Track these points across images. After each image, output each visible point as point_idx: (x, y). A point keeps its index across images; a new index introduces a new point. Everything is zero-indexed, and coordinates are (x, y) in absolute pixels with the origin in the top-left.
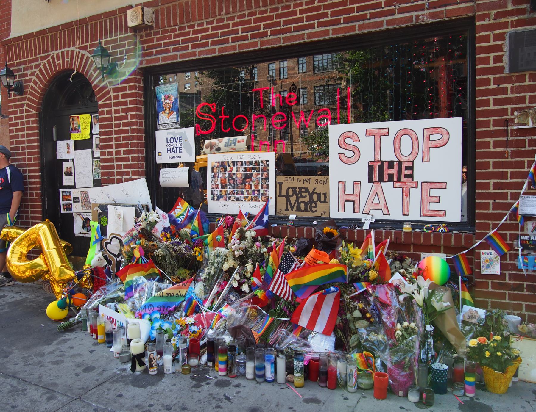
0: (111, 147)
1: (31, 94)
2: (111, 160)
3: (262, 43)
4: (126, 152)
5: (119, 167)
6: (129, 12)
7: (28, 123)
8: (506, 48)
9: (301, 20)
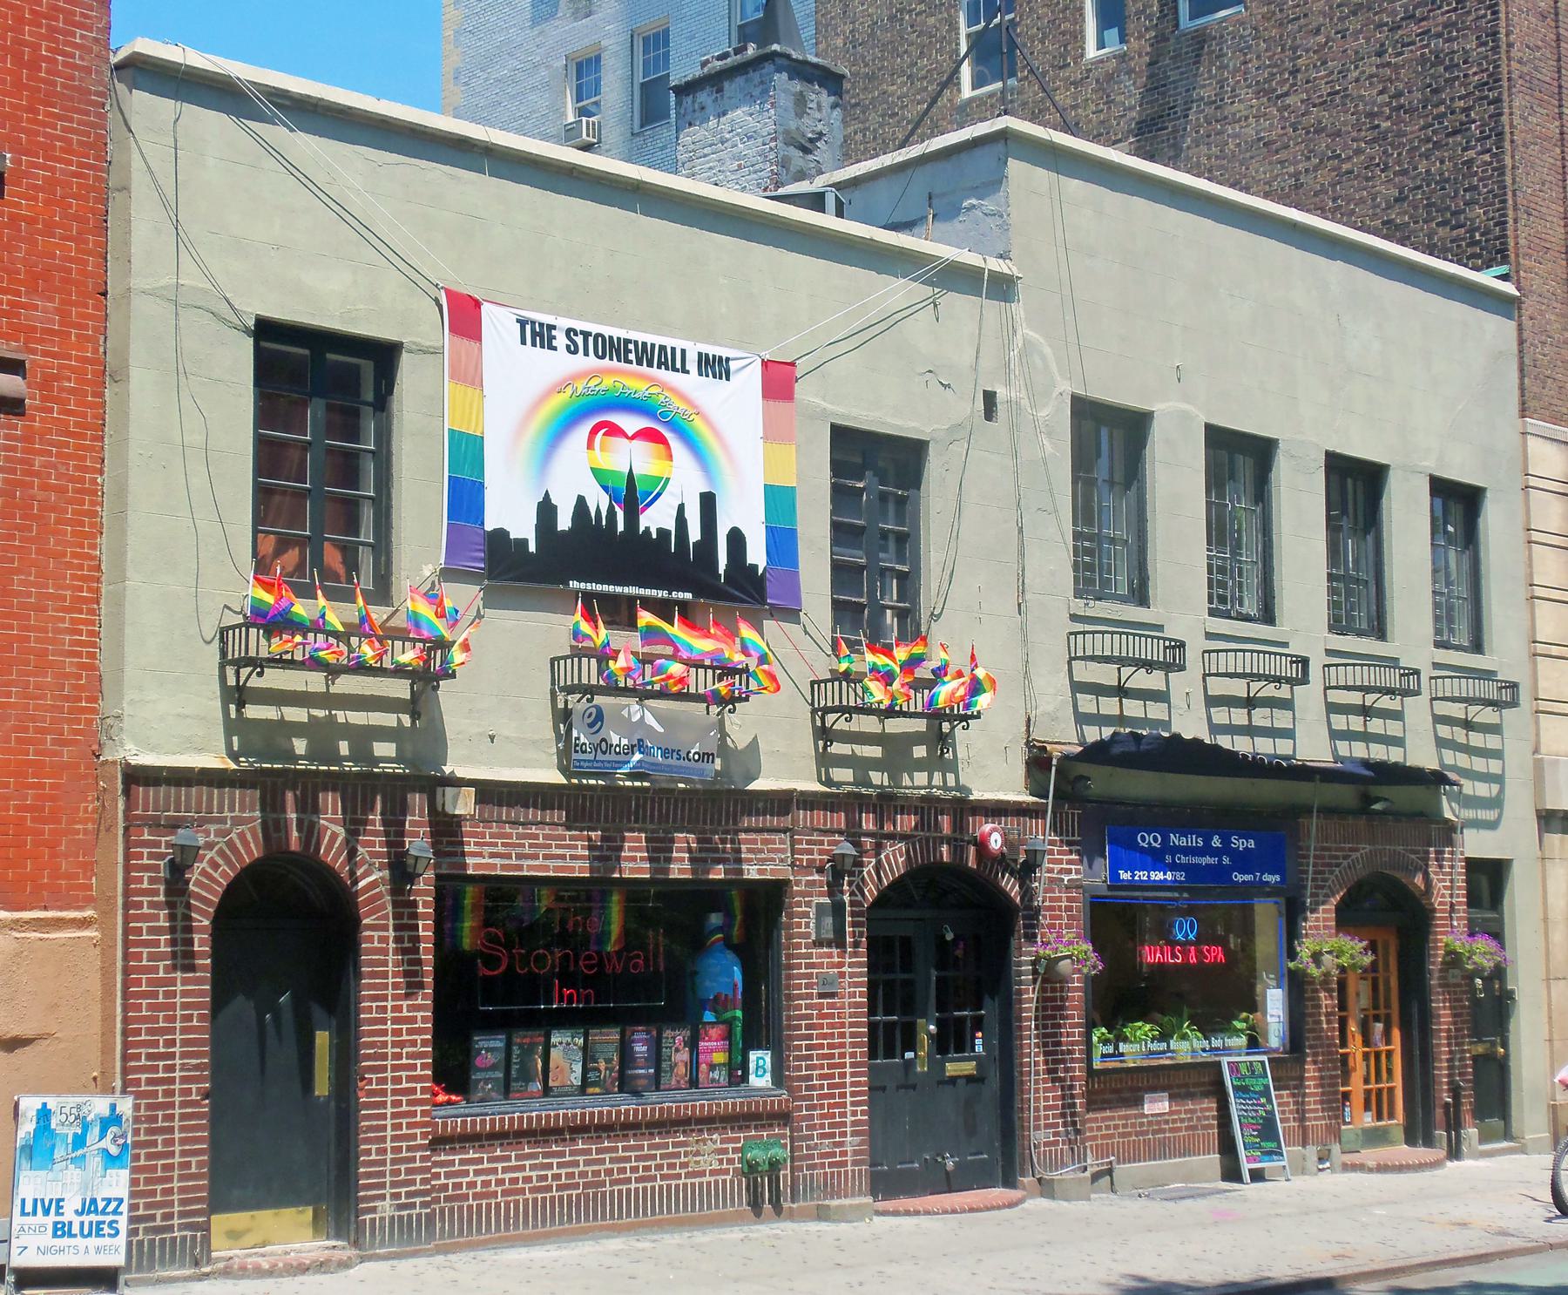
0: (385, 998)
5: (397, 1033)
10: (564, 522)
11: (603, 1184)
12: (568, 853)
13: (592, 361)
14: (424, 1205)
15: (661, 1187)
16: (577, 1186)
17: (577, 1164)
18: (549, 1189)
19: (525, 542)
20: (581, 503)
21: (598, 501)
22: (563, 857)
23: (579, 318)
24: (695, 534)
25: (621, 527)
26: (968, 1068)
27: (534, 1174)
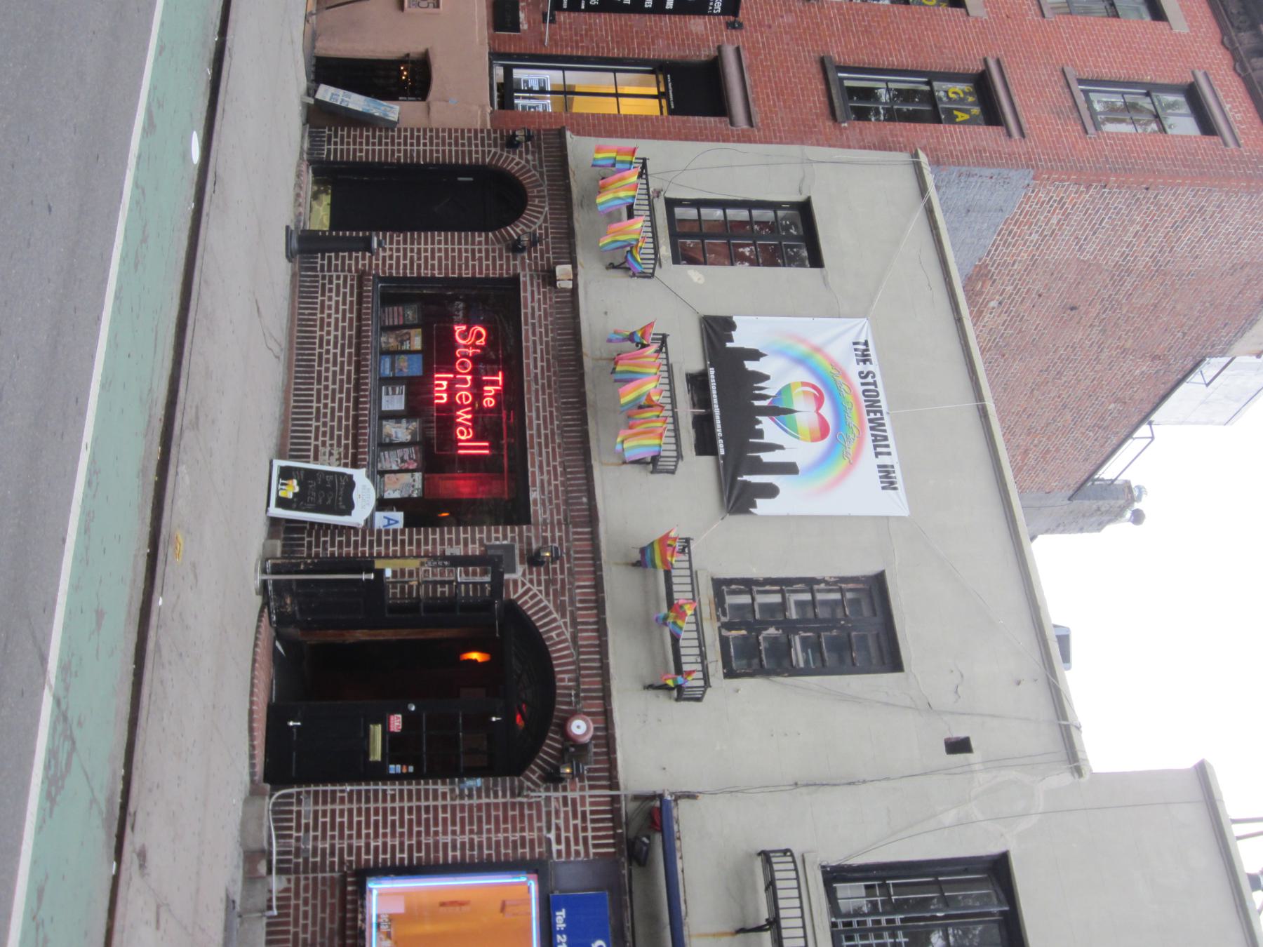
0: (446, 243)
1: (507, 157)
2: (433, 243)
3: (529, 382)
4: (440, 258)
6: (569, 267)
7: (477, 152)
8: (505, 542)
9: (544, 410)
10: (750, 365)
11: (318, 420)
12: (539, 355)
13: (860, 389)
14: (322, 266)
15: (310, 426)
16: (320, 365)
17: (337, 312)
18: (321, 346)
19: (731, 340)
20: (766, 378)
21: (770, 388)
22: (535, 352)
23: (883, 376)
24: (767, 457)
25: (757, 403)
26: (376, 755)
27: (332, 337)
